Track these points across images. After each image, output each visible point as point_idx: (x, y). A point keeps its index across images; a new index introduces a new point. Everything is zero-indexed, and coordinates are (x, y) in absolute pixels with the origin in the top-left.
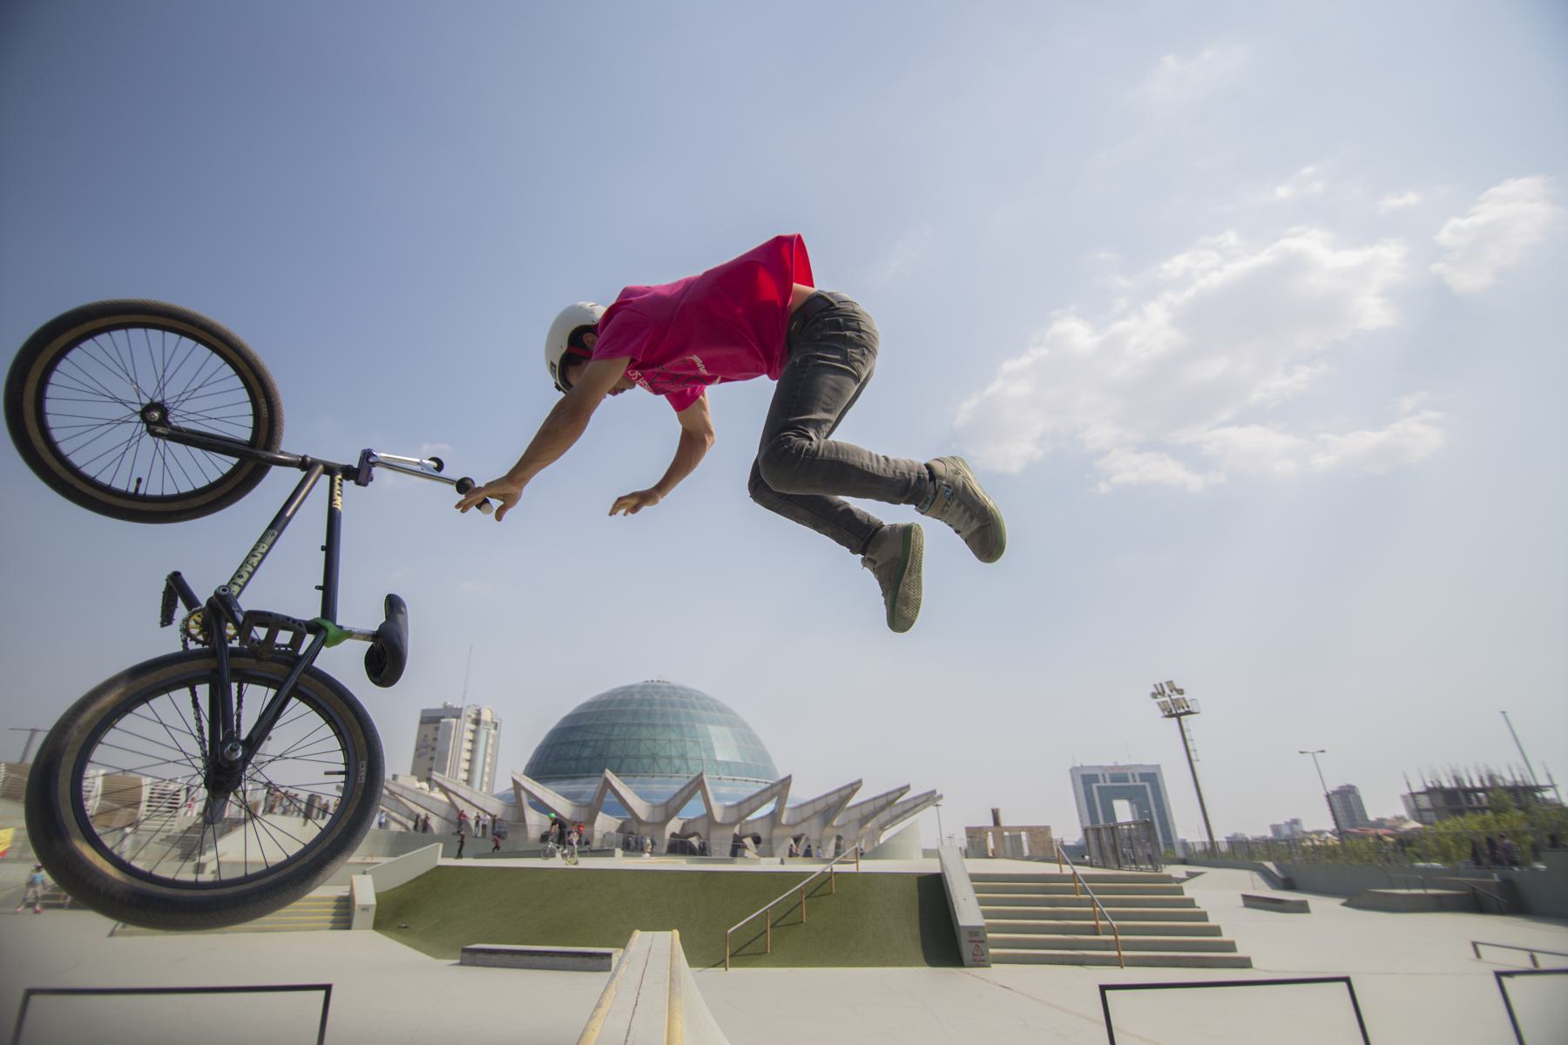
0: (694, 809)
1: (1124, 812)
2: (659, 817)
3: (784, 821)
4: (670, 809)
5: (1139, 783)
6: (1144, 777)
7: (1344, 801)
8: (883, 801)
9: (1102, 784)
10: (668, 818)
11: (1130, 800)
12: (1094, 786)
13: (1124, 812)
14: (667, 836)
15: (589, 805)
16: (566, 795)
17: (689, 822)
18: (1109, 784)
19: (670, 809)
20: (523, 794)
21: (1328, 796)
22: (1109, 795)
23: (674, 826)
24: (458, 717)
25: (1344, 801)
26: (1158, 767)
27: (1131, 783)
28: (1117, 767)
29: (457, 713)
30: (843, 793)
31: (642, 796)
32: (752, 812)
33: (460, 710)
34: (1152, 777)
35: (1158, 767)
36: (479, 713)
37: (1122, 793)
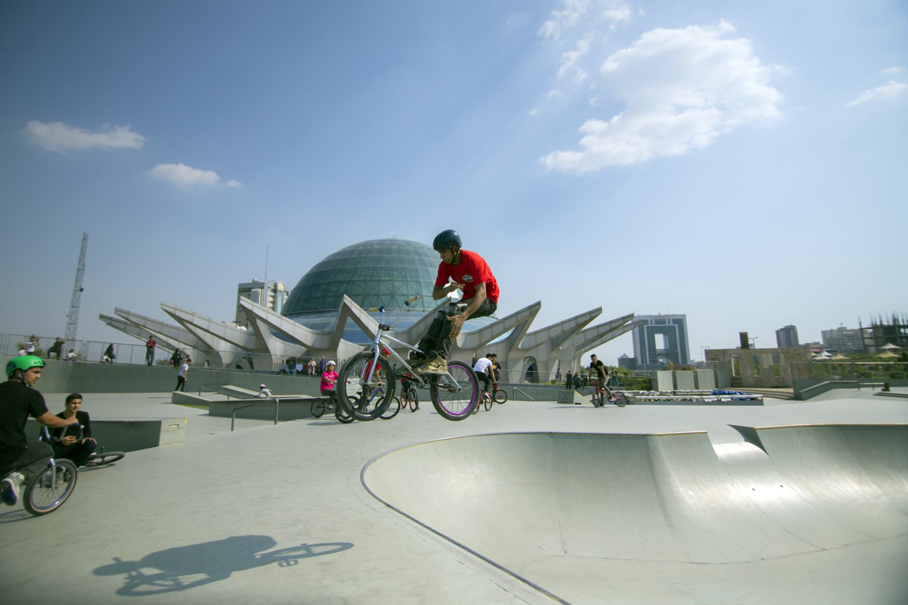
1: (660, 342)
5: (671, 324)
6: (675, 321)
7: (787, 334)
9: (650, 325)
11: (664, 334)
12: (645, 326)
13: (660, 342)
18: (654, 325)
21: (777, 332)
22: (652, 332)
24: (262, 288)
25: (787, 334)
26: (684, 316)
27: (667, 324)
28: (660, 316)
29: (262, 286)
33: (263, 284)
34: (680, 322)
35: (684, 316)
36: (276, 286)
37: (659, 332)
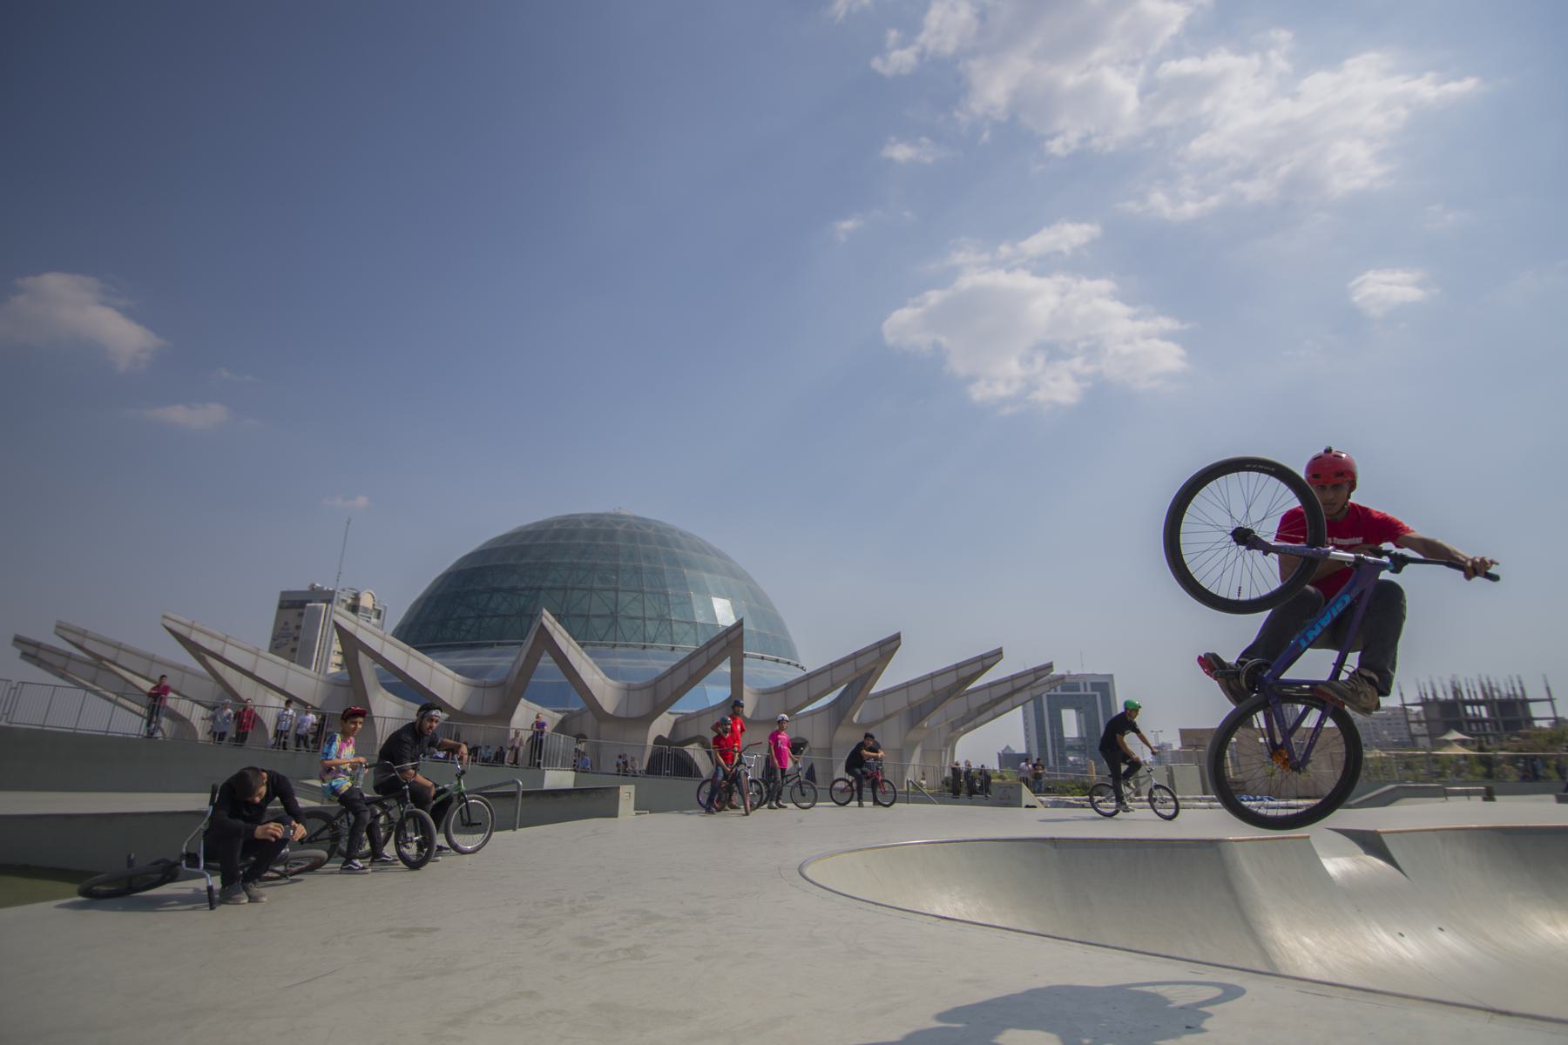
0: (714, 691)
2: (638, 709)
3: (855, 719)
4: (662, 692)
8: (1007, 688)
10: (657, 710)
14: (650, 742)
15: (501, 685)
16: (459, 671)
17: (686, 718)
19: (662, 692)
20: (363, 659)
23: (662, 726)
30: (965, 672)
31: (610, 673)
32: (811, 700)
